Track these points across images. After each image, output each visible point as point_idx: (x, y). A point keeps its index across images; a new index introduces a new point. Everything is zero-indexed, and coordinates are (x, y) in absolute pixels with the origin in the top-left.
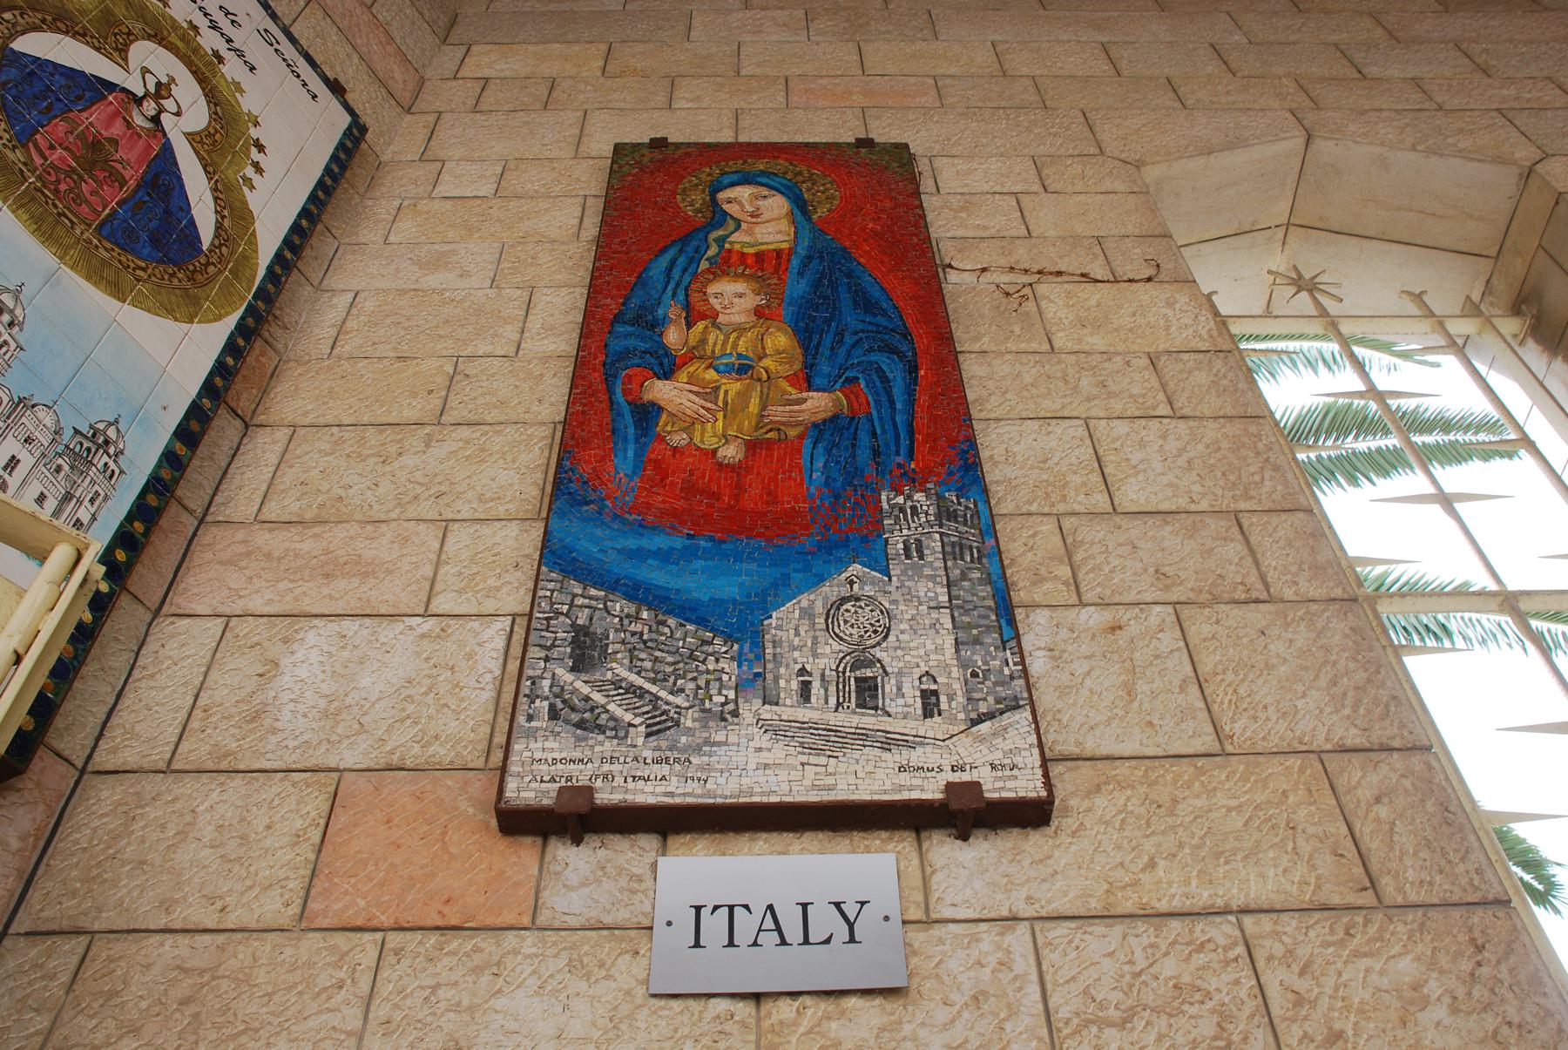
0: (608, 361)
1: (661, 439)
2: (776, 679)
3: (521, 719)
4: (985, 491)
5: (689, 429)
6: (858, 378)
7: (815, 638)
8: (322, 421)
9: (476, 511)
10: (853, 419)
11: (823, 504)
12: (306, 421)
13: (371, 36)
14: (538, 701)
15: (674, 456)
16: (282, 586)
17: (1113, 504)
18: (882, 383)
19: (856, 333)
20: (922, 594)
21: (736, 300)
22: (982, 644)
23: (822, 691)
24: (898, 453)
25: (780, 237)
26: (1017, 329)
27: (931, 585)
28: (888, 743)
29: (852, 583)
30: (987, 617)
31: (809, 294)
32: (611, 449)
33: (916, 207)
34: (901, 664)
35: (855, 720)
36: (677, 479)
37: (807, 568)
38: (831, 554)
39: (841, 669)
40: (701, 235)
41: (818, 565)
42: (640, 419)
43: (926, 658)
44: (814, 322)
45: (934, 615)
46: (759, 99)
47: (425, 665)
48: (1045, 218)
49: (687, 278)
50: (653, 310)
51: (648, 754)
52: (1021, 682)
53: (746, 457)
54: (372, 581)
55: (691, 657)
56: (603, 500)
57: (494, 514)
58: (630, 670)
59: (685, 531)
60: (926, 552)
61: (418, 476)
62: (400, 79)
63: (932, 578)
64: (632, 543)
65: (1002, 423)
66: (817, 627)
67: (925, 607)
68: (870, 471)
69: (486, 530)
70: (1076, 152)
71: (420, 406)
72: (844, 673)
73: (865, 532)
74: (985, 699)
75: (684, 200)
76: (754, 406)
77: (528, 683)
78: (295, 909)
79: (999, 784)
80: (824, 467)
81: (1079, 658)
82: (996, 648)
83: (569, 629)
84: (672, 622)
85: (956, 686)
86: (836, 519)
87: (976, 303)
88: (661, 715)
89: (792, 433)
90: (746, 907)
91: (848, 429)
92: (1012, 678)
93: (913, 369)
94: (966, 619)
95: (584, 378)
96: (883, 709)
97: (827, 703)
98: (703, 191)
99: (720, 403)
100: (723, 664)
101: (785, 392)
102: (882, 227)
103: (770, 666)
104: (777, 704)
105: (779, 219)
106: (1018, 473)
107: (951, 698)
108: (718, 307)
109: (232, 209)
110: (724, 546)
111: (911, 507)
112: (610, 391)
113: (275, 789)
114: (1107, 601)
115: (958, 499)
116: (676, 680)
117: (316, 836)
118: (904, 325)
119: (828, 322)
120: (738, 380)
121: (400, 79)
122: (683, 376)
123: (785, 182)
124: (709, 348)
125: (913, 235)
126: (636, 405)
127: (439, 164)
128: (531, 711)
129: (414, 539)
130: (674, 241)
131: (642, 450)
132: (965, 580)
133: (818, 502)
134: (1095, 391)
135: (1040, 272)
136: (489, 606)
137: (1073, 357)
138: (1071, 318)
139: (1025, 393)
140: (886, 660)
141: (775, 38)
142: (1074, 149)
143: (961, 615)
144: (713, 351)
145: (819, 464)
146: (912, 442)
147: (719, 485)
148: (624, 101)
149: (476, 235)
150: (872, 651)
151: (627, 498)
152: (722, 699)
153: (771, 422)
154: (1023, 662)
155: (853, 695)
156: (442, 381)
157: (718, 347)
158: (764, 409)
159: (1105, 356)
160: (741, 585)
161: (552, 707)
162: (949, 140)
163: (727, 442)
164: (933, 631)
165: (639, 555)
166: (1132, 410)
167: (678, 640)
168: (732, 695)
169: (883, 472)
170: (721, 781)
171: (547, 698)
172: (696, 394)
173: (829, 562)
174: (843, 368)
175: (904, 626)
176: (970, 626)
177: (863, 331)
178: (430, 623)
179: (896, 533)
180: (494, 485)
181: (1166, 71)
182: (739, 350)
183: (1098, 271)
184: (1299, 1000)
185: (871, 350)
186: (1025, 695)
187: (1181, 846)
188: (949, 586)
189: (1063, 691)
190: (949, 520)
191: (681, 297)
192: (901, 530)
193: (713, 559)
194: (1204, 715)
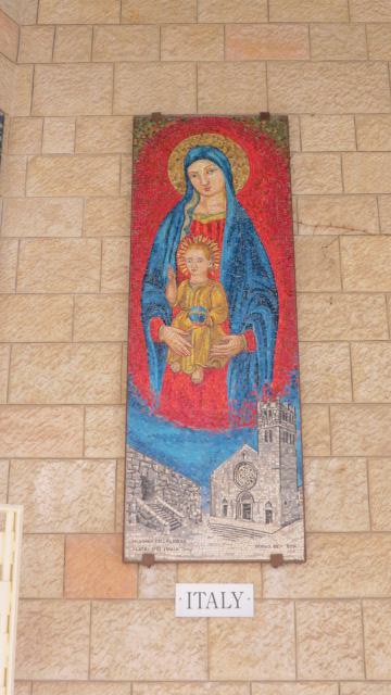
2: (216, 503)
3: (127, 522)
5: (180, 361)
8: (22, 340)
12: (15, 339)
16: (27, 443)
21: (198, 264)
28: (253, 535)
35: (241, 524)
78: (61, 591)
84: (177, 475)
89: (223, 363)
93: (276, 319)
104: (215, 516)
117: (62, 561)
123: (223, 158)
127: (40, 120)
135: (344, 227)
136: (107, 455)
145: (234, 384)
156: (69, 311)
158: (211, 347)
165: (165, 438)
176: (285, 479)
183: (373, 228)
184: (373, 632)
185: (259, 304)
187: (348, 573)
189: (318, 502)
191: (173, 262)
194: (367, 514)
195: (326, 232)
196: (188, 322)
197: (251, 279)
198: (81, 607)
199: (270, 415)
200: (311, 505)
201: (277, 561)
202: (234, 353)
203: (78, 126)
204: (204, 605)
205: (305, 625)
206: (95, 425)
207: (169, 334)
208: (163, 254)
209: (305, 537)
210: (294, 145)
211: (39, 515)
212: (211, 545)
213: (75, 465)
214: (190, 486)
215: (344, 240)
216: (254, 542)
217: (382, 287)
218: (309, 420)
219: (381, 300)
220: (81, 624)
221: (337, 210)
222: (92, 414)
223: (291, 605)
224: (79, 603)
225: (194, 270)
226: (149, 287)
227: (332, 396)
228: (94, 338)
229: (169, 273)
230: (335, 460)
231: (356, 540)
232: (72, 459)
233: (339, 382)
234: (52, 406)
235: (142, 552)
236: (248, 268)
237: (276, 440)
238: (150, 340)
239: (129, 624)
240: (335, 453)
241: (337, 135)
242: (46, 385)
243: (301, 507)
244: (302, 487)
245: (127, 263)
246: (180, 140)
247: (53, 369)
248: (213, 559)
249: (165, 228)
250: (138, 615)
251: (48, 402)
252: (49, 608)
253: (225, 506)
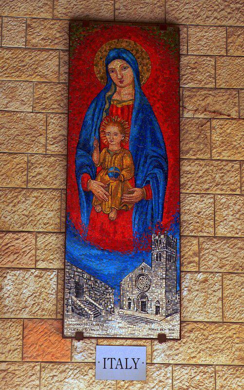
2: (123, 301)
22: (171, 292)
28: (147, 322)
29: (142, 269)
30: (174, 283)
35: (140, 315)
51: (94, 323)
52: (179, 305)
65: (190, 195)
68: (150, 225)
79: (170, 335)
89: (130, 207)
90: (115, 359)
92: (177, 303)
93: (166, 178)
107: (162, 309)
113: (9, 324)
120: (115, 180)
130: (94, 99)
135: (214, 112)
145: (136, 222)
158: (122, 196)
161: (72, 308)
170: (110, 331)
171: (71, 305)
175: (154, 285)
176: (169, 285)
183: (234, 114)
185: (155, 167)
187: (207, 348)
189: (189, 301)
191: (97, 134)
194: (221, 310)
195: (202, 116)
196: (107, 177)
197: (150, 149)
198: (34, 367)
199: (160, 243)
200: (185, 303)
201: (162, 338)
202: (137, 201)
203: (28, 26)
204: (114, 366)
205: (178, 381)
206: (43, 246)
207: (95, 186)
208: (90, 128)
209: (180, 324)
210: (183, 49)
211: (6, 306)
212: (120, 328)
213: (30, 273)
214: (107, 289)
215: (214, 122)
216: (147, 326)
217: (238, 157)
218: (185, 247)
219: (237, 166)
220: (33, 377)
221: (210, 100)
222: (41, 239)
223: (170, 368)
224: (33, 365)
225: (111, 141)
226: (80, 152)
227: (201, 231)
228: (42, 186)
229: (94, 143)
230: (201, 274)
231: (213, 327)
232: (28, 269)
233: (207, 222)
234: (14, 232)
235: (76, 331)
236: (149, 140)
237: (163, 260)
238: (81, 189)
239: (65, 378)
240: (201, 270)
241: (214, 42)
242: (9, 218)
243: (179, 305)
244: (179, 292)
245: (65, 132)
246: (103, 43)
247: (14, 206)
248: (122, 336)
249: (91, 111)
250: (71, 372)
251: (11, 230)
252: (12, 368)
253: (130, 303)
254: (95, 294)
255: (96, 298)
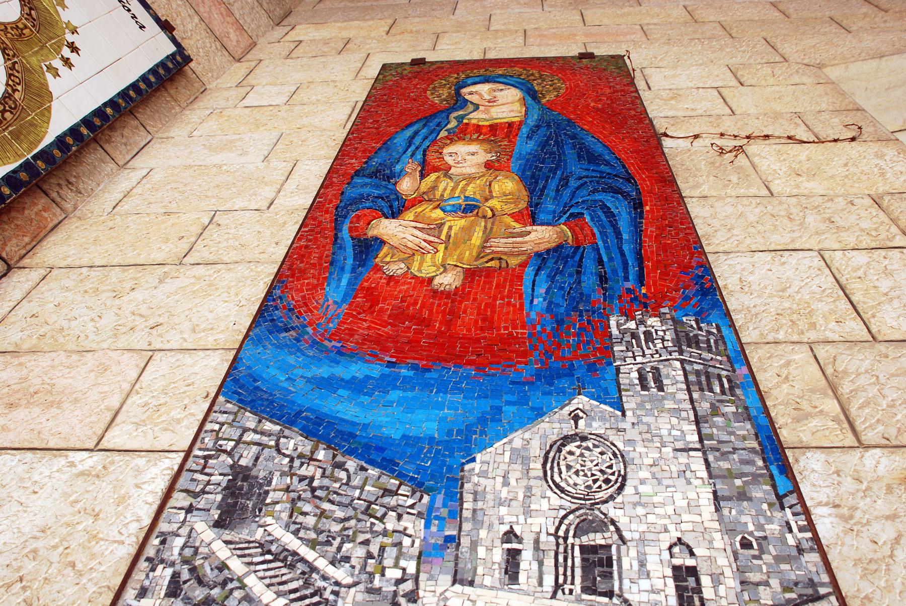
0: (342, 204)
1: (378, 269)
2: (474, 545)
4: (728, 314)
6: (583, 214)
7: (529, 488)
9: (185, 340)
10: (578, 248)
11: (544, 330)
13: (213, 8)
14: (160, 567)
15: (388, 284)
17: (870, 331)
18: (607, 217)
19: (580, 178)
20: (664, 432)
22: (750, 499)
23: (535, 566)
24: (626, 279)
25: (513, 114)
26: (734, 179)
27: (674, 421)
29: (576, 419)
31: (536, 151)
32: (325, 278)
33: (632, 92)
34: (643, 528)
36: (387, 306)
37: (523, 401)
38: (551, 384)
39: (561, 533)
40: (444, 115)
41: (536, 399)
42: (361, 252)
43: (676, 519)
44: (540, 171)
45: (683, 458)
46: (503, 42)
47: (70, 510)
48: (744, 101)
49: (427, 143)
50: (393, 165)
53: (463, 285)
54: (54, 411)
55: (367, 511)
56: (304, 326)
57: (202, 344)
58: (287, 527)
59: (387, 359)
60: (665, 382)
61: (144, 310)
62: (233, 38)
63: (676, 412)
64: (324, 371)
65: (731, 255)
66: (532, 474)
67: (669, 449)
68: (597, 296)
69: (187, 359)
70: (764, 61)
71: (168, 249)
72: (566, 538)
73: (592, 359)
74: (767, 584)
75: (432, 94)
76: (477, 239)
77: (156, 542)
80: (547, 292)
81: (877, 518)
82: (771, 505)
83: (228, 470)
85: (722, 561)
86: (559, 346)
87: (692, 160)
88: (312, 595)
89: (514, 262)
91: (573, 257)
92: (800, 550)
93: (638, 205)
94: (725, 465)
95: (314, 219)
96: (620, 596)
97: (540, 584)
98: (450, 88)
99: (443, 237)
100: (407, 523)
101: (508, 227)
102: (603, 105)
103: (467, 526)
104: (471, 583)
105: (512, 103)
106: (758, 301)
107: (717, 580)
108: (451, 162)
109: (27, 87)
110: (428, 375)
111: (645, 333)
112: (337, 229)
114: (895, 443)
115: (697, 324)
116: (342, 542)
118: (627, 171)
119: (554, 171)
120: (462, 217)
121: (233, 38)
122: (410, 215)
124: (438, 194)
125: (630, 109)
126: (359, 240)
128: (147, 583)
129: (114, 369)
130: (420, 119)
131: (356, 278)
132: (717, 415)
133: (539, 328)
134: (822, 227)
137: (794, 200)
138: (784, 169)
139: (752, 230)
140: (623, 522)
141: (518, 10)
142: (762, 59)
143: (717, 459)
144: (442, 195)
145: (541, 290)
146: (641, 269)
147: (431, 311)
148: (399, 47)
149: (263, 128)
150: (603, 508)
151: (331, 325)
152: (398, 574)
153: (493, 252)
154: (811, 526)
155: (578, 572)
157: (448, 192)
158: (486, 241)
159: (826, 198)
160: (442, 420)
161: (175, 576)
162: (656, 58)
163: (445, 271)
164: (683, 480)
165: (329, 384)
166: (866, 242)
167: (355, 488)
168: (411, 567)
169: (611, 298)
171: (173, 564)
172: (420, 229)
173: (549, 393)
174: (567, 206)
175: (644, 474)
176: (729, 475)
177: (587, 177)
178: (95, 459)
179: (629, 361)
180: (210, 316)
181: (827, 13)
182: (467, 194)
183: (802, 134)
185: (595, 191)
186: (825, 578)
188: (697, 422)
190: (689, 346)
191: (419, 156)
192: (634, 357)
193: (413, 389)
253: (513, 556)
254: (323, 514)
255: (319, 532)
